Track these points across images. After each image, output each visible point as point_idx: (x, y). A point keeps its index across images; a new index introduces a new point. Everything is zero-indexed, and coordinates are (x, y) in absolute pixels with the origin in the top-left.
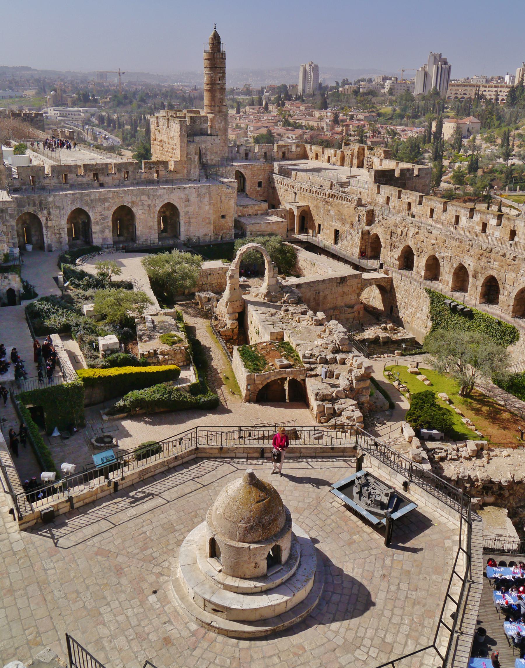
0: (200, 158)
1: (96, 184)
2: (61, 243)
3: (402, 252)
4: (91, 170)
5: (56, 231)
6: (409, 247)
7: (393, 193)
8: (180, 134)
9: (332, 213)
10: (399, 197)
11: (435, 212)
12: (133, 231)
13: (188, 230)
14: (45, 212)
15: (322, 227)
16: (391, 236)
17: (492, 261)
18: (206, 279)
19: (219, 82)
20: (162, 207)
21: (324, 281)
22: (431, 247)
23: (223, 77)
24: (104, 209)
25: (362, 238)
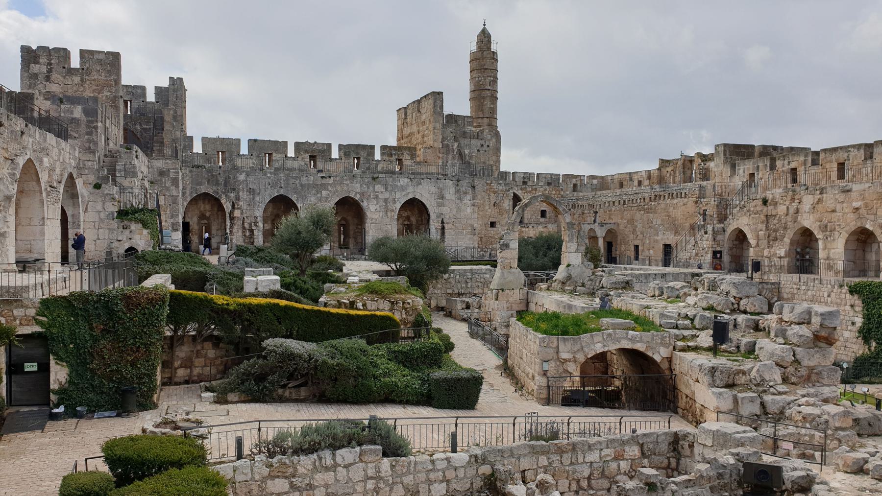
3: (792, 243)
4: (307, 151)
7: (761, 165)
8: (434, 111)
9: (657, 221)
10: (773, 167)
12: (362, 242)
14: (232, 195)
15: (640, 248)
16: (768, 222)
18: (464, 285)
19: (489, 88)
22: (851, 216)
23: (495, 80)
24: (320, 200)
25: (714, 239)
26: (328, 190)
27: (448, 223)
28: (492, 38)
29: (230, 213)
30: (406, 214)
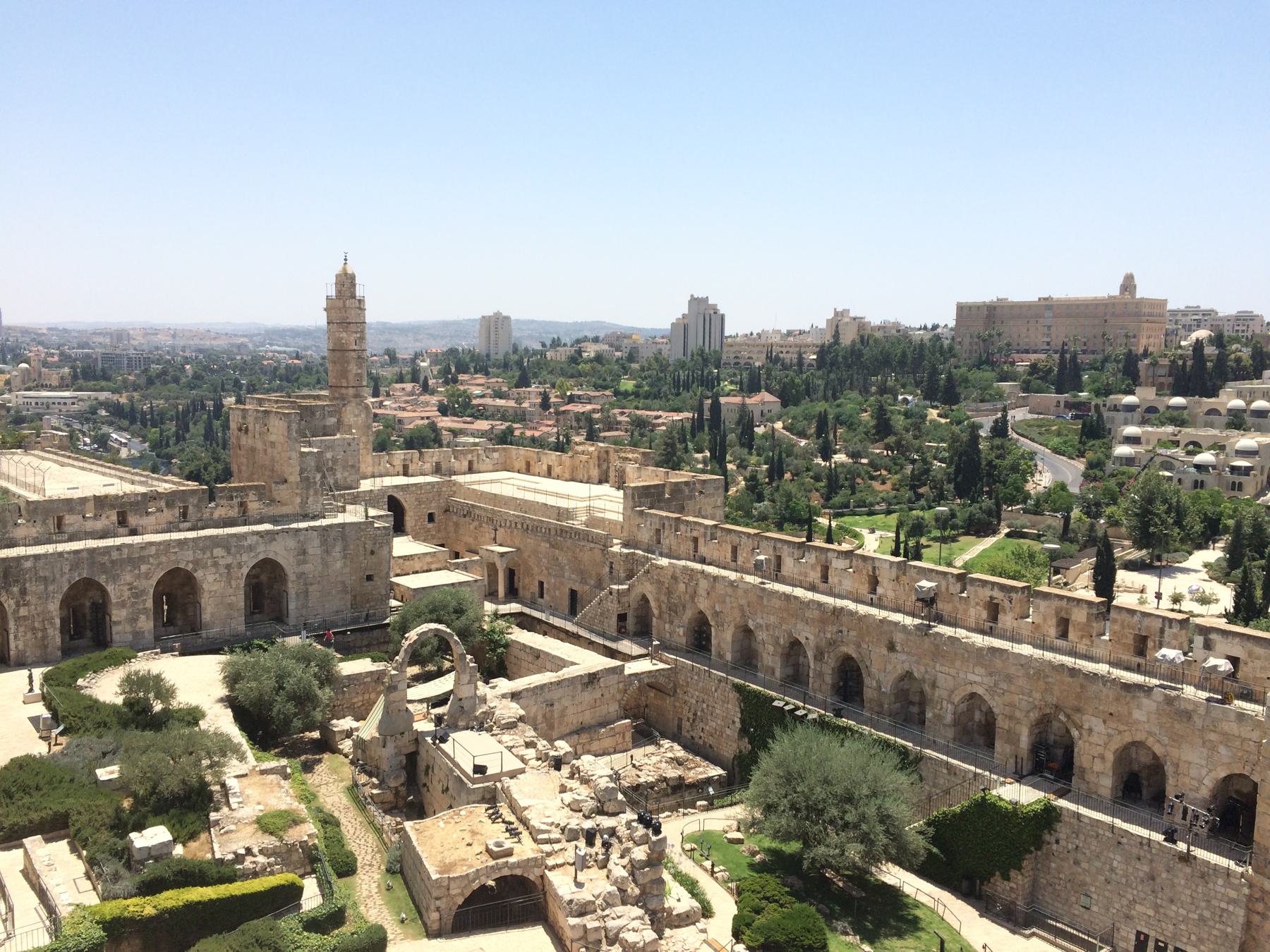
0: (324, 477)
1: (121, 530)
2: (46, 647)
3: (690, 623)
4: (113, 507)
5: (36, 625)
6: (701, 612)
7: (667, 523)
9: (563, 559)
11: (739, 552)
12: (195, 615)
13: (305, 606)
14: (15, 589)
15: (545, 585)
17: (845, 629)
19: (355, 347)
20: (254, 567)
21: (559, 683)
22: (737, 614)
23: (362, 338)
24: (138, 577)
26: (149, 563)
27: (311, 584)
28: (357, 281)
29: (16, 611)
30: (254, 571)
